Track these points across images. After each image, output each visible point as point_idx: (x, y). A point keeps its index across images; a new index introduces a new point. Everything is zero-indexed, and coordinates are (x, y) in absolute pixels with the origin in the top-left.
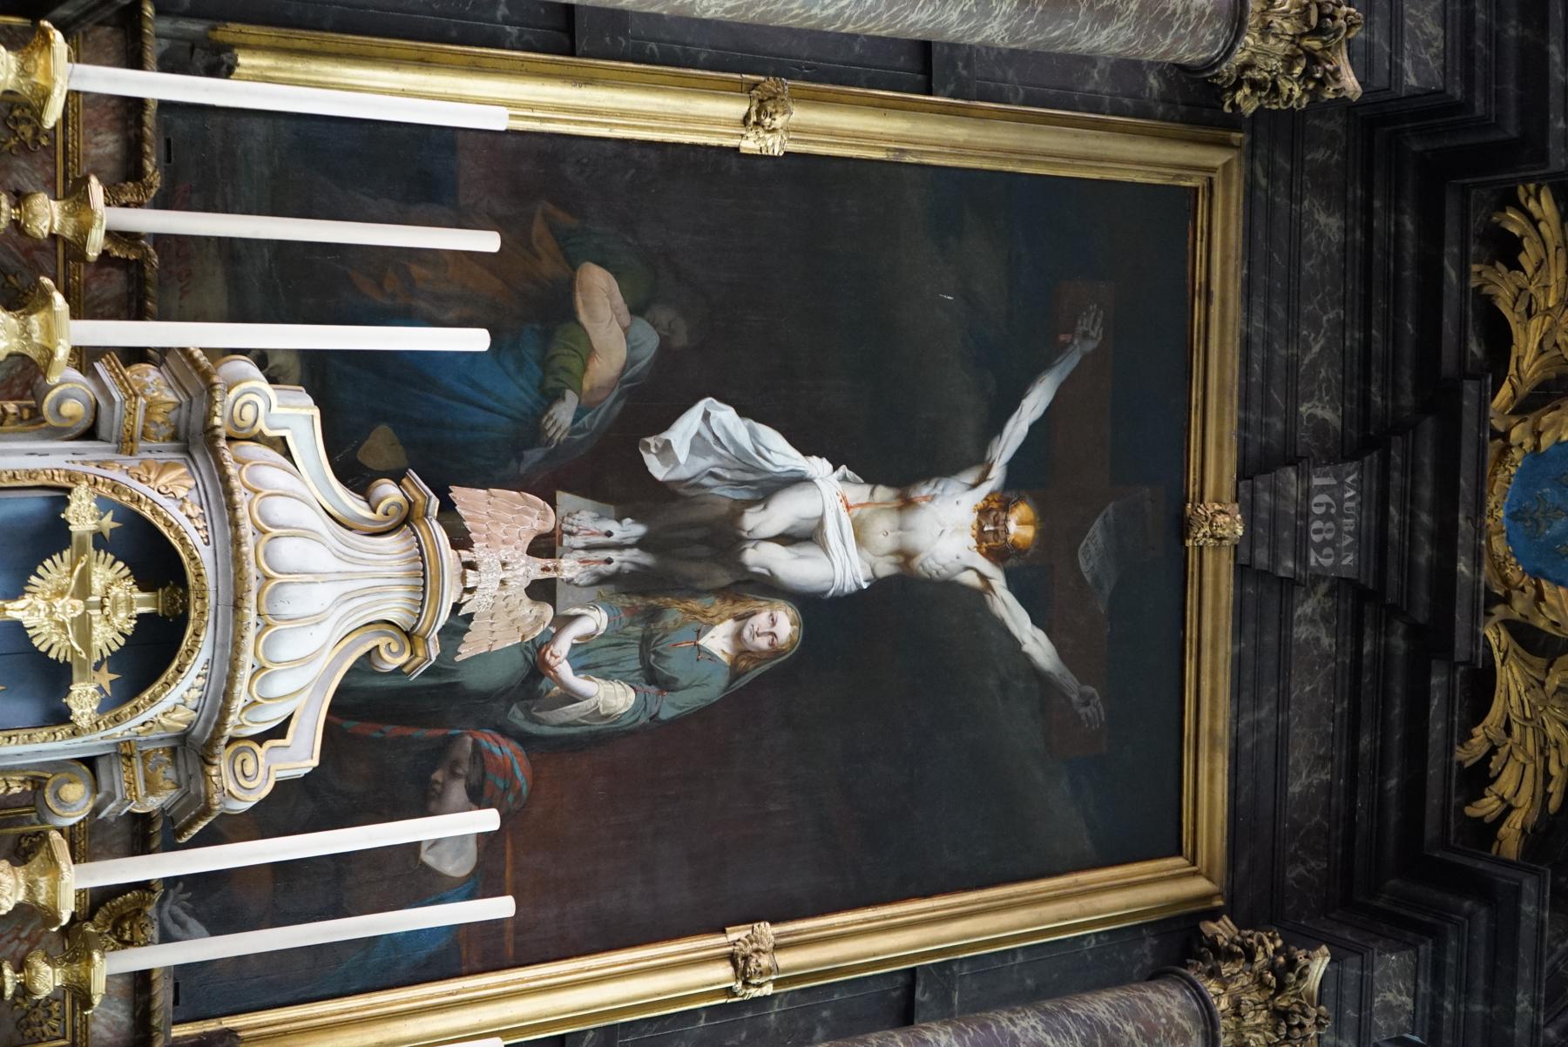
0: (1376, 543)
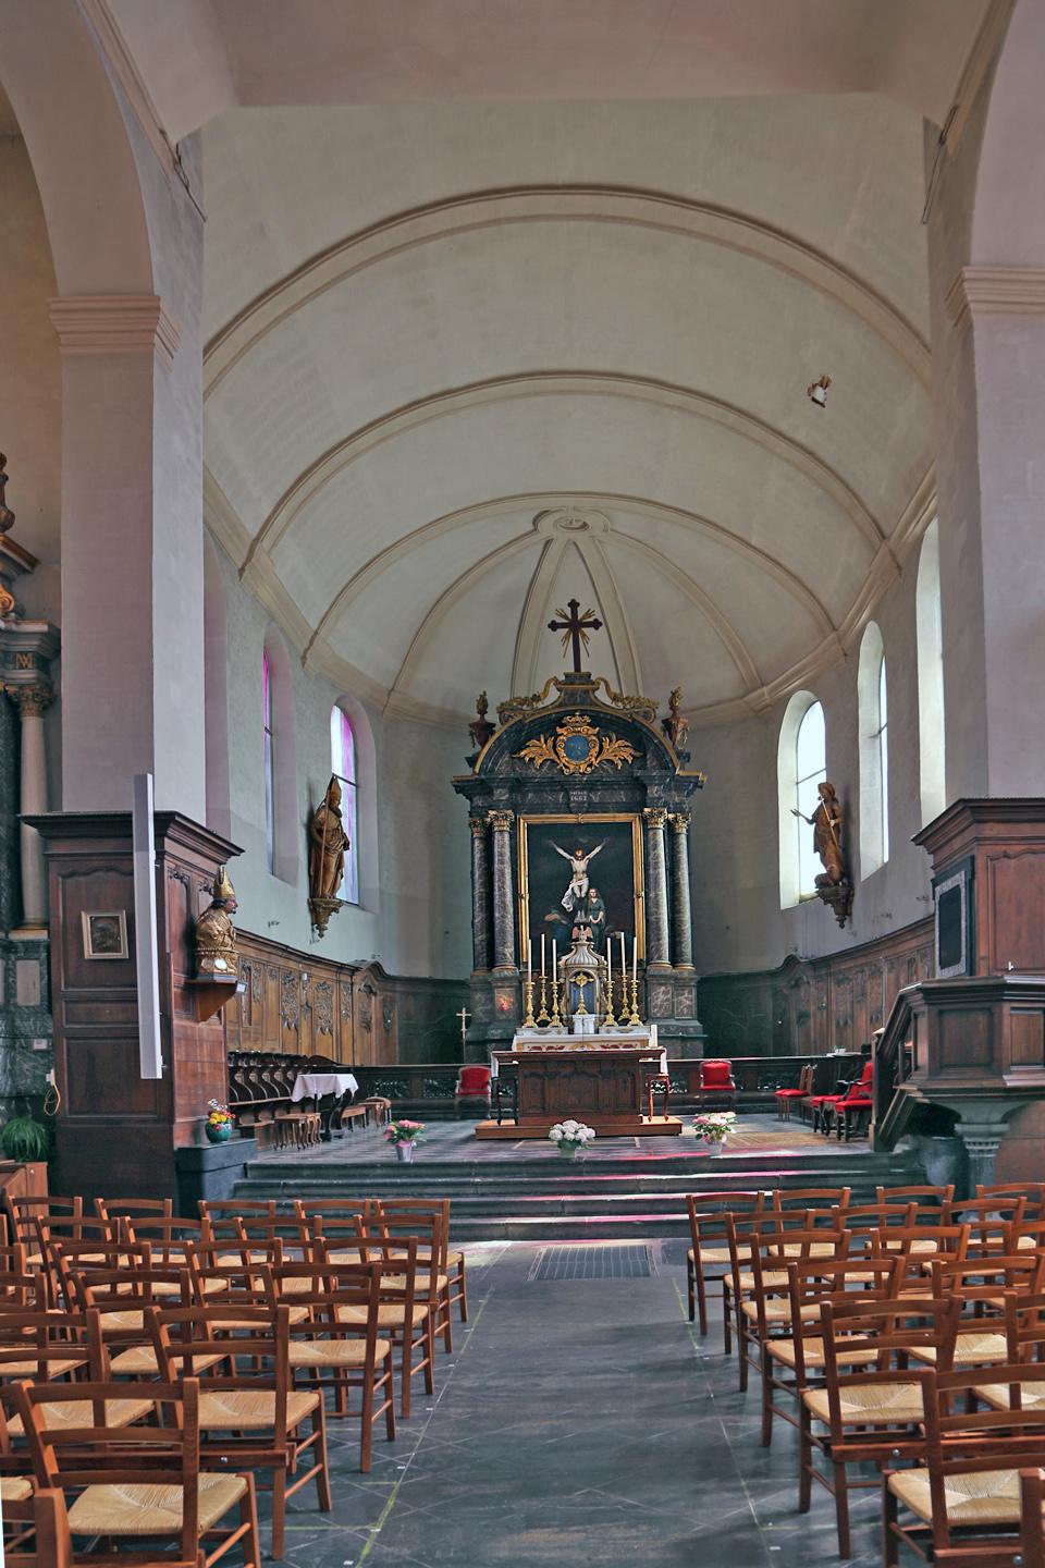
0: (582, 790)
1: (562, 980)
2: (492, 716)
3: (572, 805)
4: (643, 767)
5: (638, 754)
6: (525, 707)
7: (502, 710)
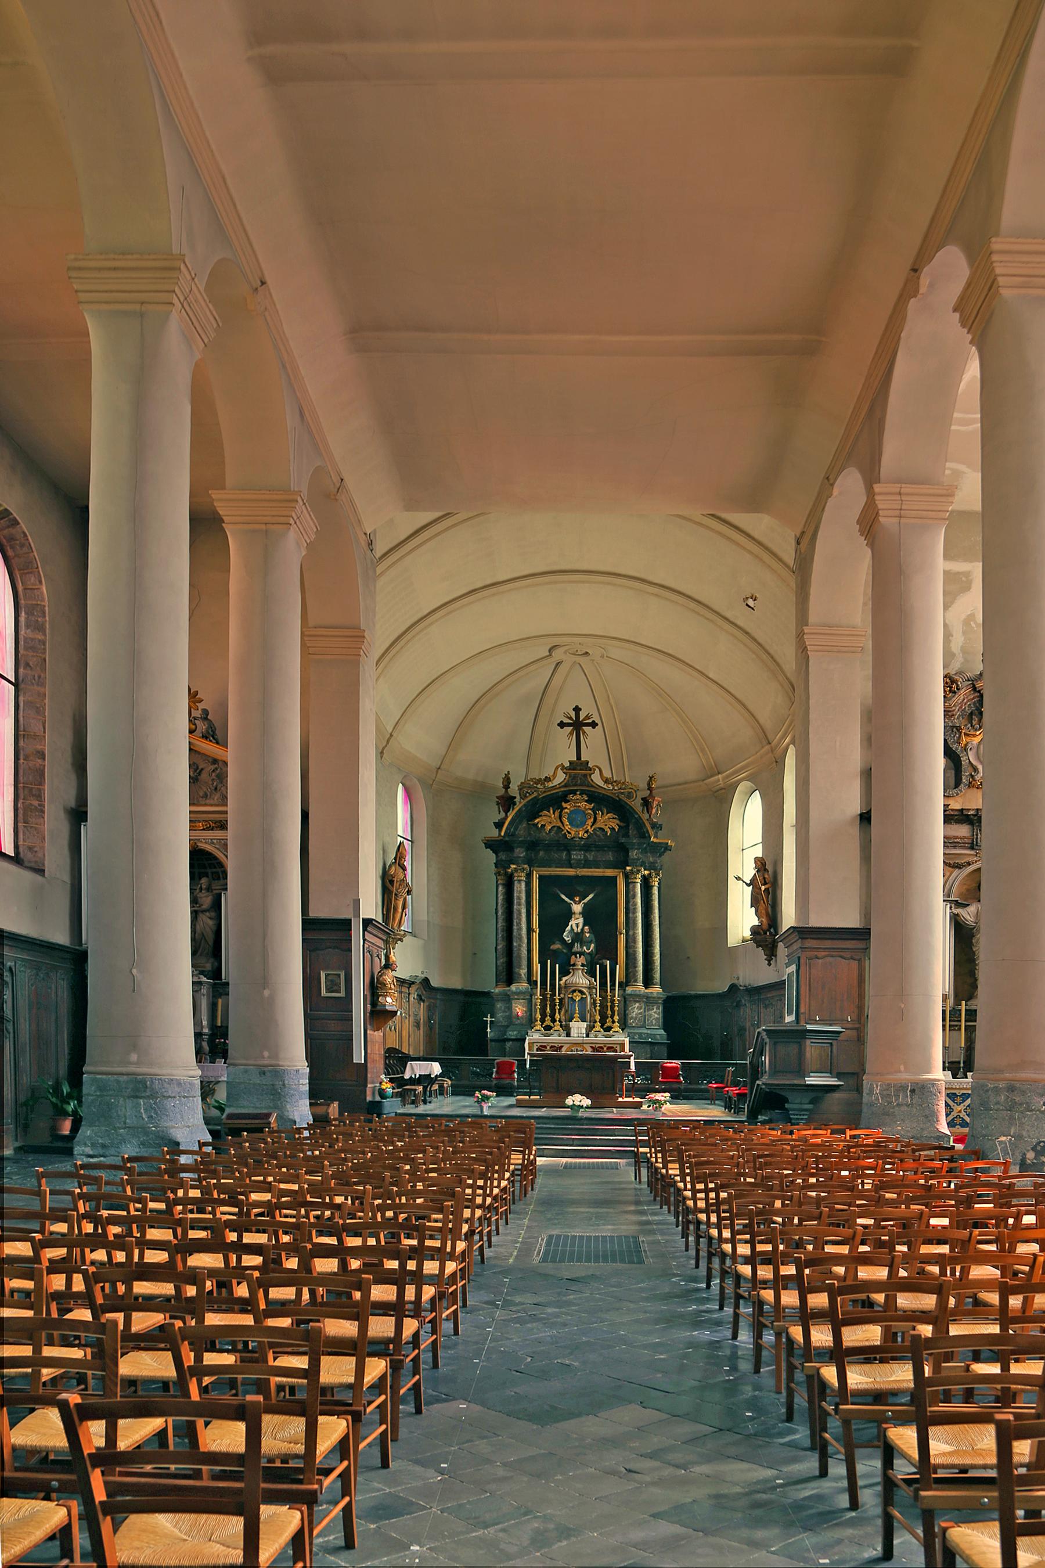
0: (580, 850)
1: (562, 996)
2: (514, 790)
3: (572, 862)
4: (626, 835)
5: (622, 824)
6: (539, 786)
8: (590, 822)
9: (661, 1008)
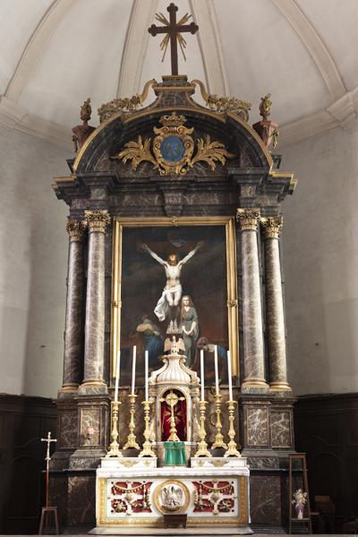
0: (177, 191)
6: (125, 109)
7: (103, 112)
8: (189, 152)
9: (291, 417)
